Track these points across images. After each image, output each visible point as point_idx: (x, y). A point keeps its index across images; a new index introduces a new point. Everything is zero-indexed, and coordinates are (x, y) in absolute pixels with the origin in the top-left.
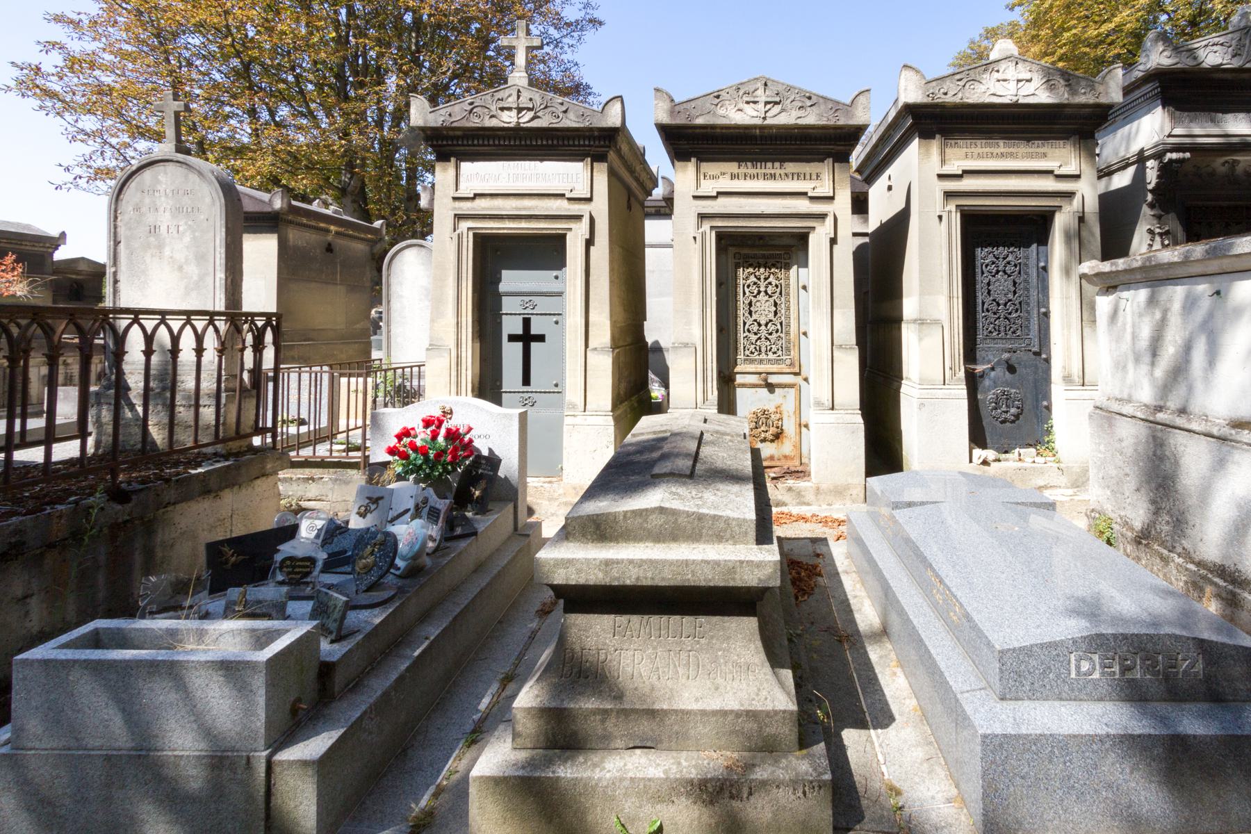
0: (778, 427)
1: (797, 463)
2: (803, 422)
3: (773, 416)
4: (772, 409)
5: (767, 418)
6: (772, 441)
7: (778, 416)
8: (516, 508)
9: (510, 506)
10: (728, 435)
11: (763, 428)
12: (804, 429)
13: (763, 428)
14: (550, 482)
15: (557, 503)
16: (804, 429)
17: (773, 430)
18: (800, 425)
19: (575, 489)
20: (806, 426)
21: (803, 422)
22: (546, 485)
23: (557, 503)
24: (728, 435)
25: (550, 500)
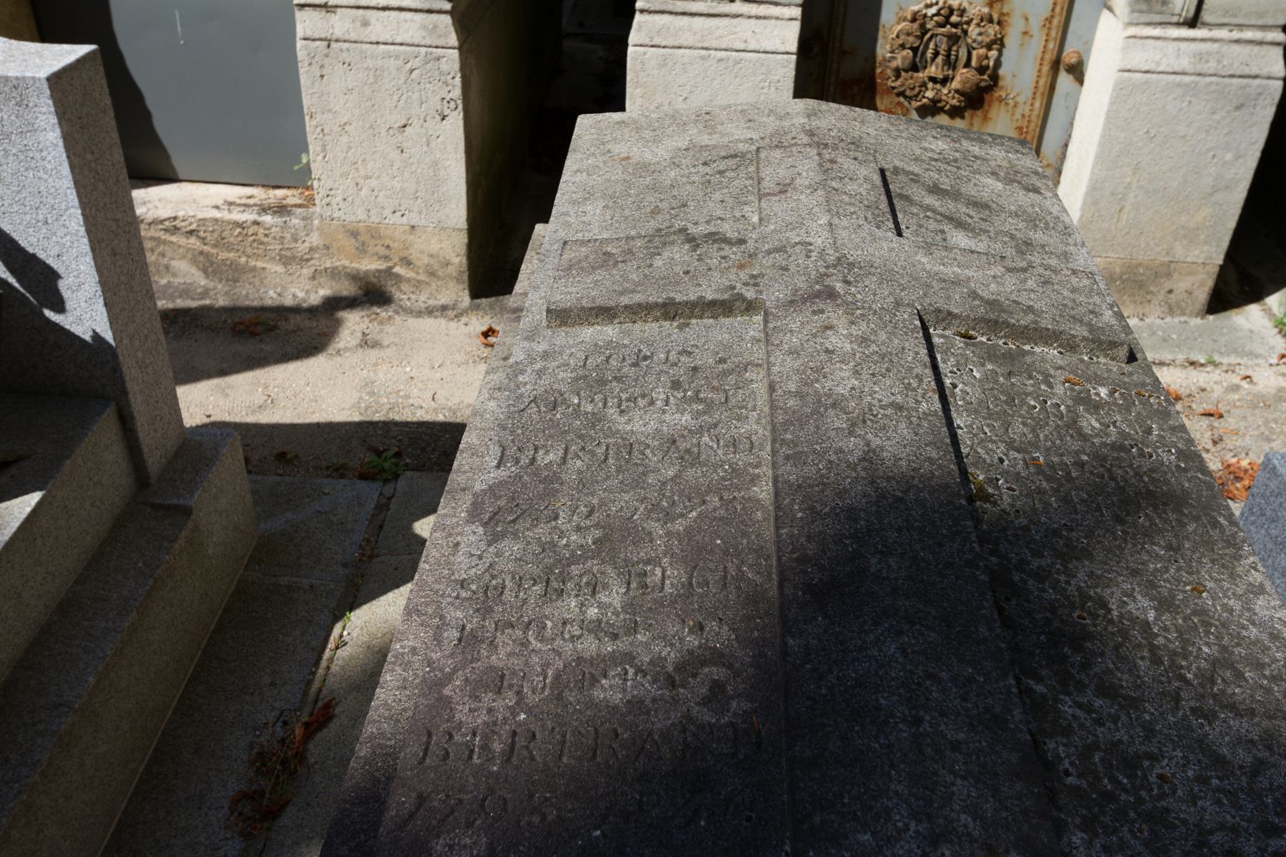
0: (981, 70)
2: (1069, 57)
3: (973, 31)
4: (977, 8)
5: (954, 40)
6: (955, 113)
7: (992, 30)
8: (126, 421)
9: (105, 430)
10: (1048, 337)
11: (933, 70)
12: (1064, 80)
13: (933, 70)
14: (281, 209)
15: (307, 272)
16: (1064, 80)
17: (963, 77)
18: (1056, 65)
19: (355, 234)
20: (1077, 71)
21: (1069, 57)
22: (267, 219)
23: (307, 272)
25: (286, 260)
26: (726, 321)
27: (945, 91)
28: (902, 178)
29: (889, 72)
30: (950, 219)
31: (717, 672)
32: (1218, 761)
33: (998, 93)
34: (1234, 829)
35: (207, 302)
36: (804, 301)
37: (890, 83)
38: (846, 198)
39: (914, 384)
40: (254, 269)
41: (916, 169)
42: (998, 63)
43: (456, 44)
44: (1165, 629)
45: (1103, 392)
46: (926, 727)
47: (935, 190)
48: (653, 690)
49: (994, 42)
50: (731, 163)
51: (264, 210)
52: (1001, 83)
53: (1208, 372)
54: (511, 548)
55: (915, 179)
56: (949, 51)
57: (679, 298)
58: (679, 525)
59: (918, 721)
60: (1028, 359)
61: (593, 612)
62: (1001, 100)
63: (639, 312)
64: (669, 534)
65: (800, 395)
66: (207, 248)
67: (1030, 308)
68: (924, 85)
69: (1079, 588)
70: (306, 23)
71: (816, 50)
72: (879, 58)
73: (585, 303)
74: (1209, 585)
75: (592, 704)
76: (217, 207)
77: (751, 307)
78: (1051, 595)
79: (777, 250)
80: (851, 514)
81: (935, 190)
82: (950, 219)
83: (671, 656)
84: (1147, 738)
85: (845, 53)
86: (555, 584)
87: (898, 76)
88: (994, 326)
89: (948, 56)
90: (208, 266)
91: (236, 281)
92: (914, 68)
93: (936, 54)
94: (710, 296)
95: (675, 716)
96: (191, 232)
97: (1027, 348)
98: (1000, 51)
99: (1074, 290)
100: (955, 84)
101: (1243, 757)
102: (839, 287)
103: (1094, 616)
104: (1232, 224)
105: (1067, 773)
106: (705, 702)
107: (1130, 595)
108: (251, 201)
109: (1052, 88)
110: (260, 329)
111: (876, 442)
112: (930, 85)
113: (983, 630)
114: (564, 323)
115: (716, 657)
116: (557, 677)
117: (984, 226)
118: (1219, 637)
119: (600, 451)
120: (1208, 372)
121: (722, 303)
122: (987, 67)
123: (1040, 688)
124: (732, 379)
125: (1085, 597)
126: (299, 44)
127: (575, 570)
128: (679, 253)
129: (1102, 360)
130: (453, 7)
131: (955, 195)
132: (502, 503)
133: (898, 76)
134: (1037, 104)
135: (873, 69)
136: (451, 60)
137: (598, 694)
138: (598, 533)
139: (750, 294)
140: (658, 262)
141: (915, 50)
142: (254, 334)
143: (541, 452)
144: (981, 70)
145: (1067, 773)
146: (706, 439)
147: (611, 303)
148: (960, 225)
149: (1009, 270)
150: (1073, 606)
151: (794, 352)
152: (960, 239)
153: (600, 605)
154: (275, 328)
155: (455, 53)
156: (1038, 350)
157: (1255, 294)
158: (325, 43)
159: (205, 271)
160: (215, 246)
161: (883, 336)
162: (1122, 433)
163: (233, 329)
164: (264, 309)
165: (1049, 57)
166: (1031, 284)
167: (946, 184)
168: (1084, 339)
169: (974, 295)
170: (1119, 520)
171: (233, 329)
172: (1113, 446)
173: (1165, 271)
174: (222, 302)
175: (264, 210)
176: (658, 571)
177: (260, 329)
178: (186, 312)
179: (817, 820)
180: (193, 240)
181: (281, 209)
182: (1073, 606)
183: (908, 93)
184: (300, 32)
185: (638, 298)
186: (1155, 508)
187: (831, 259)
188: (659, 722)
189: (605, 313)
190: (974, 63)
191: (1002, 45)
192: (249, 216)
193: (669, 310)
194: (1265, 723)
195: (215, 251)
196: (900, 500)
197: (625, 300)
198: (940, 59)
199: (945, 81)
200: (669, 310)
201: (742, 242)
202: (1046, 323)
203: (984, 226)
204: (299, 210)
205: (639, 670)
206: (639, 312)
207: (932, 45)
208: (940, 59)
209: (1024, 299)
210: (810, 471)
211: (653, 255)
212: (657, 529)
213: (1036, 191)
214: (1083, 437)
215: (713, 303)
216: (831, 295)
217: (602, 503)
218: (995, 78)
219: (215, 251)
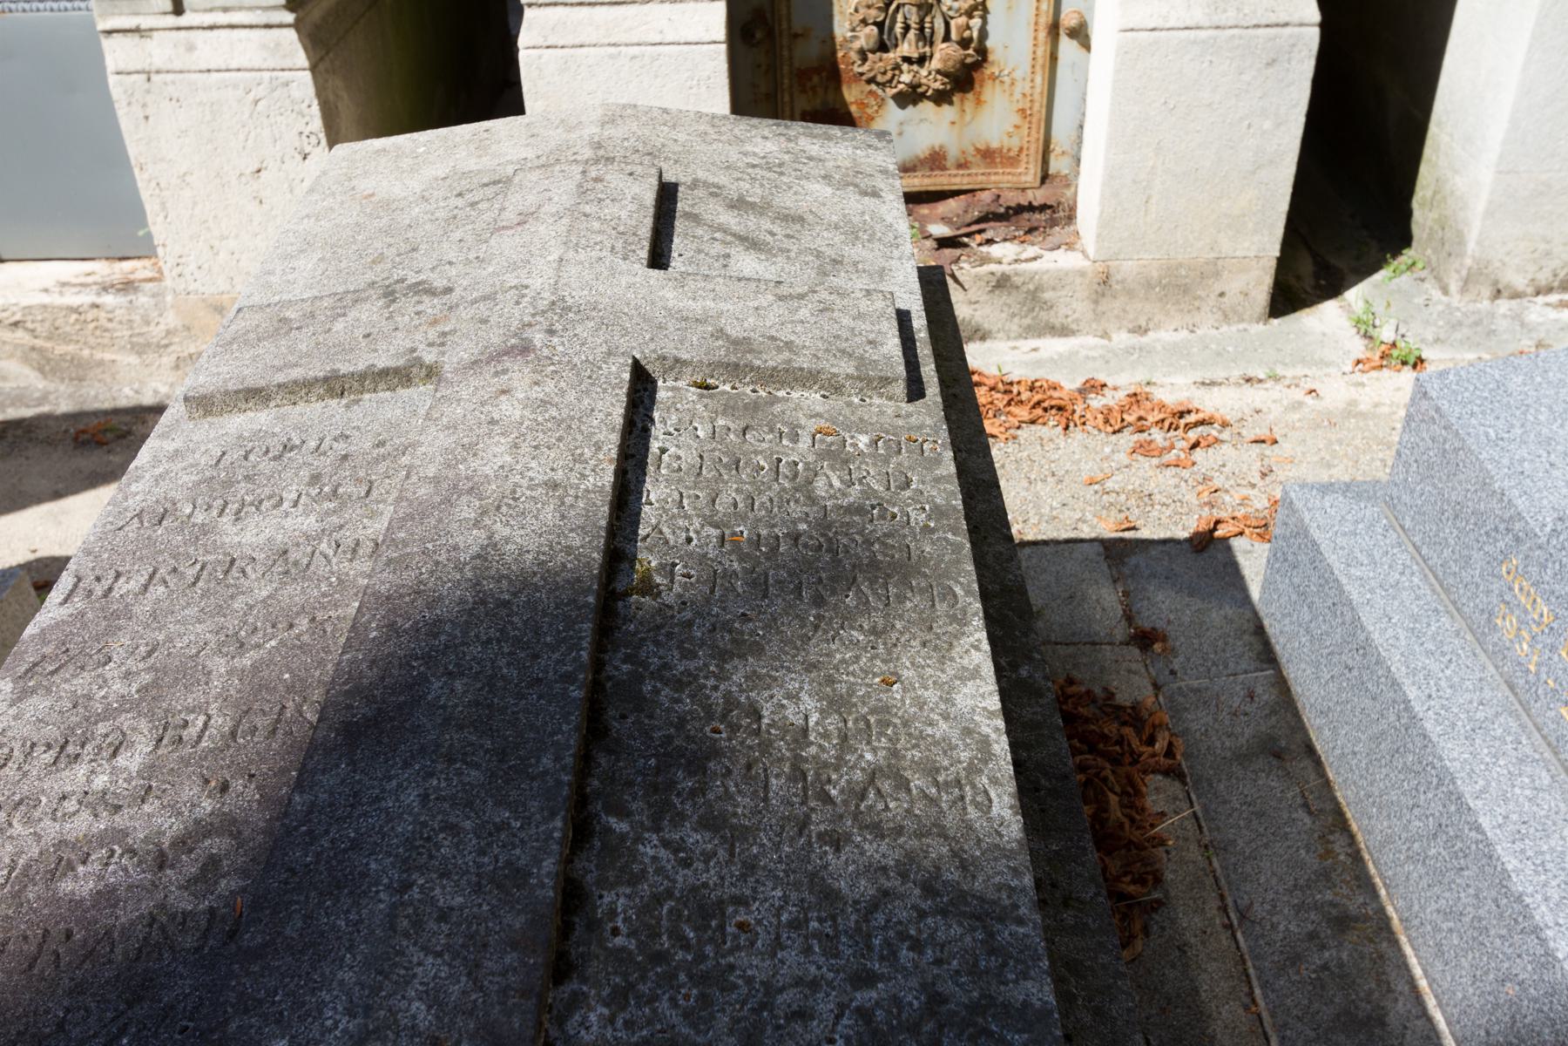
0: (965, 43)
1: (1028, 173)
6: (941, 98)
10: (807, 379)
11: (908, 48)
12: (1067, 46)
13: (908, 48)
14: (128, 286)
15: (168, 360)
16: (1067, 46)
17: (944, 54)
18: (1054, 29)
20: (1080, 34)
21: (1068, 19)
22: (109, 299)
23: (168, 360)
24: (807, 379)
25: (140, 349)
26: (403, 393)
27: (924, 72)
28: (700, 192)
29: (854, 56)
30: (742, 239)
31: (215, 845)
32: (830, 896)
33: (989, 70)
34: (814, 985)
35: (45, 409)
36: (491, 359)
37: (857, 69)
38: (596, 225)
39: (588, 453)
40: (101, 363)
41: (722, 179)
42: (983, 34)
43: (306, 64)
44: (826, 735)
45: (863, 440)
46: (415, 893)
47: (739, 204)
48: (137, 876)
49: (974, 8)
50: (490, 191)
51: (105, 288)
52: (991, 57)
53: (1267, 389)
54: (38, 705)
55: (716, 191)
56: (921, 22)
57: (344, 368)
58: (247, 661)
59: (406, 886)
60: (777, 408)
61: (100, 781)
62: (994, 78)
63: (298, 390)
64: (230, 673)
65: (436, 480)
66: (39, 343)
67: (789, 345)
68: (897, 67)
69: (728, 696)
70: (117, 53)
71: (759, 35)
72: (839, 39)
73: (231, 386)
74: (907, 674)
75: (56, 900)
76: (46, 290)
77: (432, 373)
78: (687, 704)
79: (485, 298)
80: (434, 628)
81: (739, 204)
82: (742, 239)
83: (171, 827)
84: (743, 877)
85: (796, 36)
86: (70, 749)
87: (864, 60)
88: (735, 370)
89: (921, 29)
90: (46, 364)
91: (81, 380)
92: (882, 47)
93: (907, 28)
94: (382, 362)
95: (147, 906)
96: (16, 324)
97: (781, 394)
98: (984, 18)
99: (860, 316)
100: (935, 64)
101: (866, 889)
102: (538, 338)
103: (734, 728)
104: (1284, 206)
105: (615, 932)
106: (189, 884)
107: (794, 697)
108: (90, 280)
109: (1054, 58)
110: (109, 436)
111: (501, 531)
112: (905, 67)
113: (547, 761)
114: (208, 413)
115: (226, 825)
116: (28, 867)
117: (787, 244)
118: (893, 740)
119: (191, 573)
120: (1267, 389)
121: (397, 371)
122: (971, 39)
123: (621, 826)
124: (382, 467)
125: (731, 702)
126: (112, 80)
127: (102, 728)
128: (369, 313)
129: (877, 401)
130: (297, 20)
131: (760, 209)
132: (48, 650)
133: (864, 60)
134: (1038, 79)
135: (834, 52)
136: (303, 84)
137: (66, 886)
138: (147, 678)
139: (429, 357)
140: (339, 326)
141: (880, 25)
142: (100, 444)
143: (122, 580)
144: (965, 43)
145: (615, 932)
146: (324, 546)
147: (262, 383)
148: (752, 244)
149: (781, 298)
150: (710, 716)
151: (452, 427)
152: (747, 263)
153: (114, 771)
154: (129, 433)
155: (307, 76)
156: (795, 395)
157: (1331, 286)
158: (144, 77)
159: (41, 370)
160: (49, 338)
161: (571, 396)
162: (868, 492)
163: (76, 439)
164: (116, 412)
165: (1045, 20)
166: (804, 313)
167: (755, 194)
168: (848, 376)
169: (720, 333)
170: (818, 601)
171: (76, 439)
172: (849, 510)
173: (1213, 270)
174: (65, 407)
175: (105, 288)
176: (202, 718)
177: (109, 436)
178: (18, 424)
179: (233, 1026)
180: (20, 333)
181: (128, 286)
182: (710, 716)
183: (880, 79)
184: (111, 64)
185: (296, 373)
186: (873, 582)
187: (542, 305)
188: (126, 915)
189: (255, 395)
190: (954, 35)
191: (986, 10)
192: (85, 298)
193: (335, 386)
194: (914, 843)
195: (48, 345)
196: (506, 604)
197: (280, 378)
198: (912, 34)
199: (922, 60)
200: (335, 386)
201: (448, 290)
202: (803, 362)
203: (787, 244)
204: (151, 285)
205: (132, 852)
206: (298, 390)
207: (900, 18)
208: (912, 34)
209: (785, 335)
210: (409, 577)
211: (335, 318)
212: (219, 665)
213: (875, 194)
214: (812, 500)
215: (385, 373)
216: (525, 349)
217: (170, 639)
218: (983, 52)
219: (48, 345)
